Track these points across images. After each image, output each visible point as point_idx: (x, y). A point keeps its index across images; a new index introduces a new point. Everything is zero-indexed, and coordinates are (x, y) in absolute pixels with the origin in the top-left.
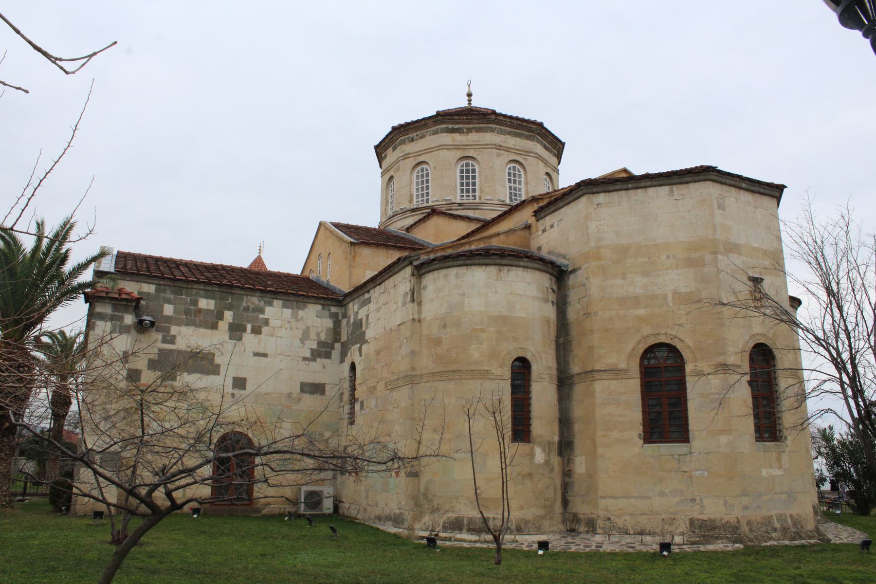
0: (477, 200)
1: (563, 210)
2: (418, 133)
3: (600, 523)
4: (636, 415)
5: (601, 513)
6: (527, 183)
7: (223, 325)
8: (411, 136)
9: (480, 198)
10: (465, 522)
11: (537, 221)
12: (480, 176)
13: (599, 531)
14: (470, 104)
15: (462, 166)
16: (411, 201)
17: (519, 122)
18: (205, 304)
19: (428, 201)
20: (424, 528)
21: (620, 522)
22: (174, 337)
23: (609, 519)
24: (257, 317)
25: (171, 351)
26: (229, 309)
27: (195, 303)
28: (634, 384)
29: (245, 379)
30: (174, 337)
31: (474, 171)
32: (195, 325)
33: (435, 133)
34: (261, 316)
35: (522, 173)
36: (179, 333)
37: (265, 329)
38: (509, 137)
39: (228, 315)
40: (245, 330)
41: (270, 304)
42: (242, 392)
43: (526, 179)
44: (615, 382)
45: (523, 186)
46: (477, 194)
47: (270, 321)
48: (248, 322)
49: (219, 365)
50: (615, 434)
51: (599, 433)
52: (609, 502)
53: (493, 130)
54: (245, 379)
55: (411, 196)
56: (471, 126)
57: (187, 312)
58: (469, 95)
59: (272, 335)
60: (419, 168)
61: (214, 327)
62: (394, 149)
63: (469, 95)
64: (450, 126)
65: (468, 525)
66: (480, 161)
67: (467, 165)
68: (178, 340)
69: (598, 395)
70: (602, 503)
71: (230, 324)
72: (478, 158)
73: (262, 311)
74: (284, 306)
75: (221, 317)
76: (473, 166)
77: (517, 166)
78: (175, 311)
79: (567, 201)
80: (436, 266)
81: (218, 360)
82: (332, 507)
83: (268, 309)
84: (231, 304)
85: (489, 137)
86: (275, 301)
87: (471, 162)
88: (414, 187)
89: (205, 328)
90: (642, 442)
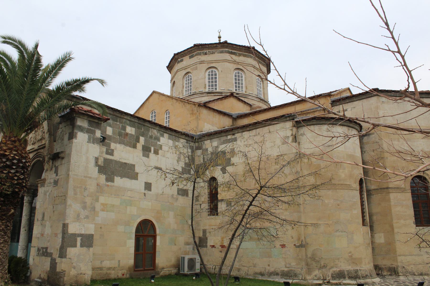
0: (244, 93)
1: (354, 103)
2: (210, 51)
3: (400, 270)
4: (411, 212)
5: (399, 264)
7: (139, 146)
8: (205, 51)
9: (246, 92)
10: (346, 273)
11: (332, 107)
12: (245, 80)
13: (400, 274)
15: (236, 73)
16: (205, 88)
18: (130, 130)
19: (216, 89)
20: (315, 278)
21: (409, 269)
22: (113, 150)
23: (404, 267)
24: (157, 143)
25: (111, 160)
26: (142, 136)
27: (124, 128)
28: (409, 195)
29: (151, 183)
30: (113, 150)
32: (124, 144)
33: (222, 52)
34: (158, 143)
36: (116, 149)
37: (160, 152)
39: (142, 139)
40: (150, 151)
41: (163, 136)
42: (149, 192)
43: (263, 86)
44: (400, 194)
45: (262, 90)
46: (244, 89)
47: (163, 147)
48: (152, 146)
49: (137, 174)
50: (402, 221)
51: (394, 221)
52: (402, 258)
53: (251, 57)
54: (151, 183)
55: (205, 85)
56: (241, 53)
57: (120, 135)
58: (220, 37)
59: (164, 156)
60: (210, 70)
61: (135, 147)
62: (190, 57)
63: (220, 37)
64: (230, 51)
65: (348, 274)
67: (238, 73)
68: (115, 153)
69: (392, 201)
70: (399, 259)
71: (143, 145)
73: (159, 140)
74: (169, 138)
75: (138, 140)
78: (114, 133)
79: (361, 98)
80: (314, 123)
81: (137, 170)
82: (199, 268)
83: (161, 138)
84: (143, 132)
86: (165, 134)
87: (240, 72)
88: (207, 80)
89: (130, 147)
90: (415, 226)
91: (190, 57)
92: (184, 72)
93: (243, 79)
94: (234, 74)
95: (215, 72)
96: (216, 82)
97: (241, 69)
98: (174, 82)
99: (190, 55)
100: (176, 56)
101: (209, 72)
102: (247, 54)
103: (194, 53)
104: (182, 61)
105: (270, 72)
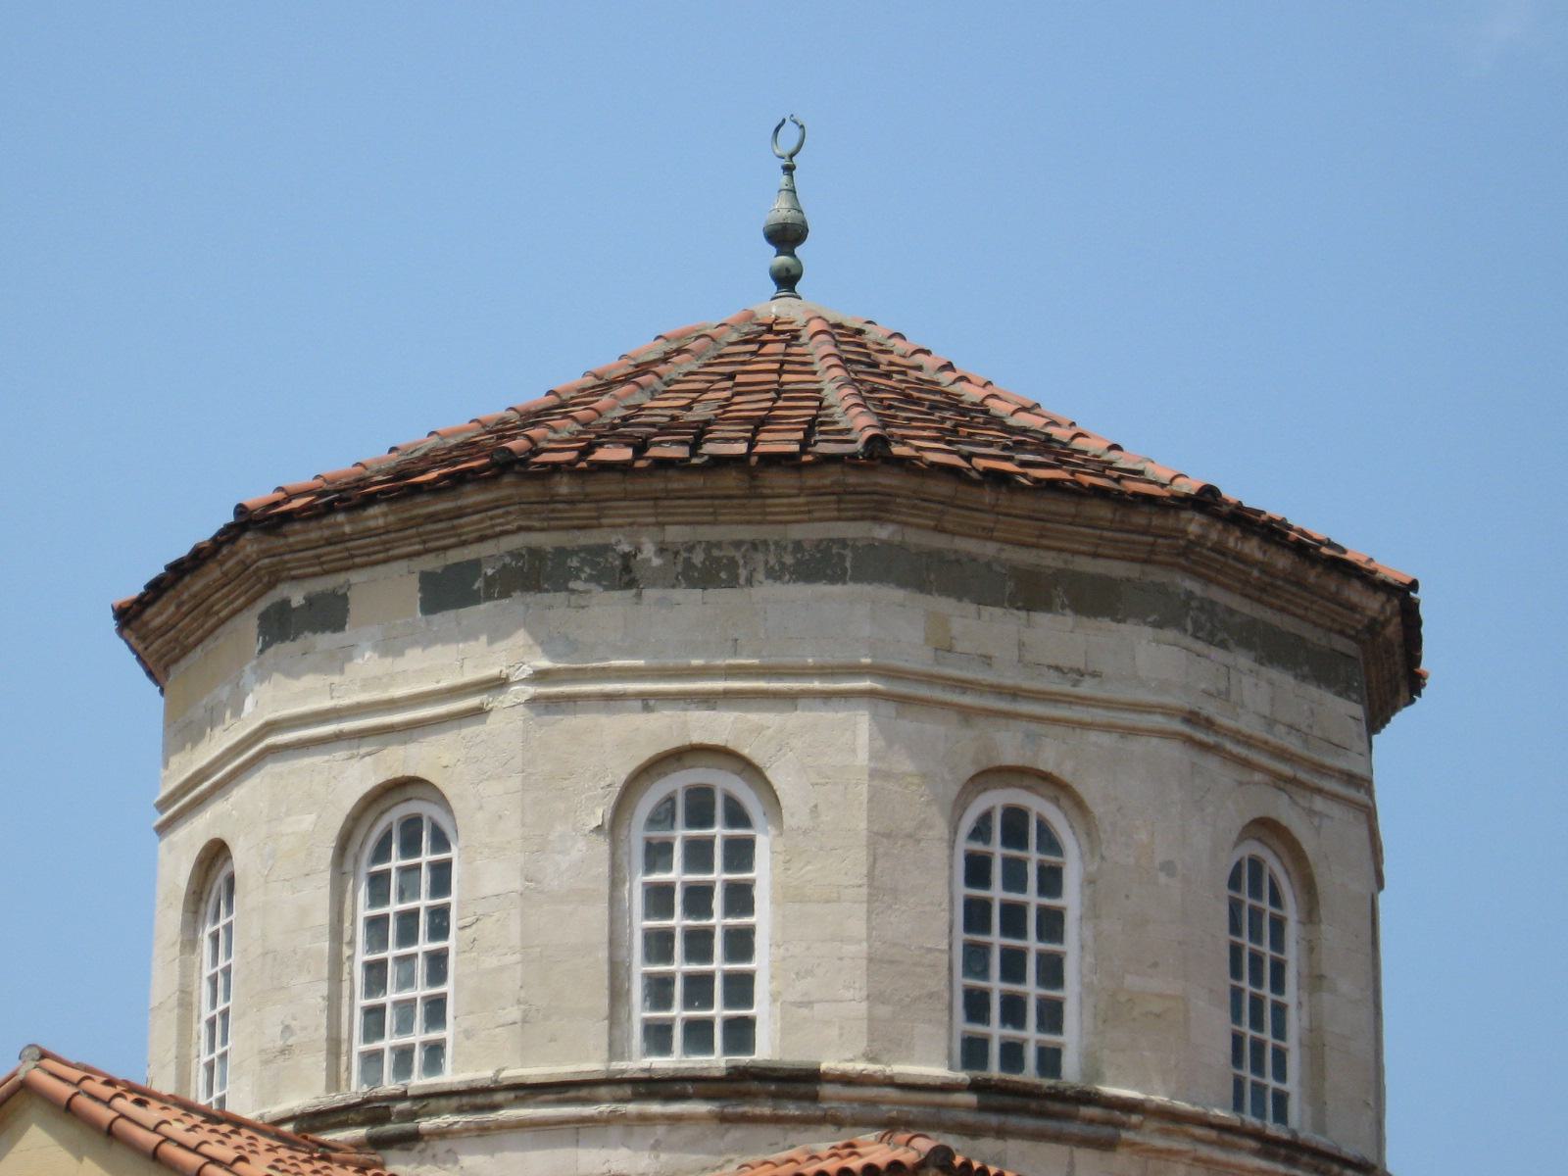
2: (675, 534)
6: (1315, 981)
12: (1092, 911)
14: (786, 281)
17: (1283, 561)
19: (741, 1033)
31: (1051, 881)
33: (818, 565)
35: (1291, 912)
38: (1243, 660)
43: (1311, 948)
60: (677, 782)
66: (1098, 809)
67: (1015, 826)
72: (1089, 788)
76: (1049, 841)
77: (1273, 865)
85: (1148, 660)
87: (1036, 805)
91: (428, 581)
92: (357, 776)
93: (1071, 899)
94: (963, 845)
95: (737, 815)
96: (741, 943)
97: (1045, 777)
98: (216, 853)
99: (432, 563)
100: (249, 545)
101: (663, 816)
102: (1118, 569)
103: (491, 553)
104: (329, 614)
105: (1415, 683)
